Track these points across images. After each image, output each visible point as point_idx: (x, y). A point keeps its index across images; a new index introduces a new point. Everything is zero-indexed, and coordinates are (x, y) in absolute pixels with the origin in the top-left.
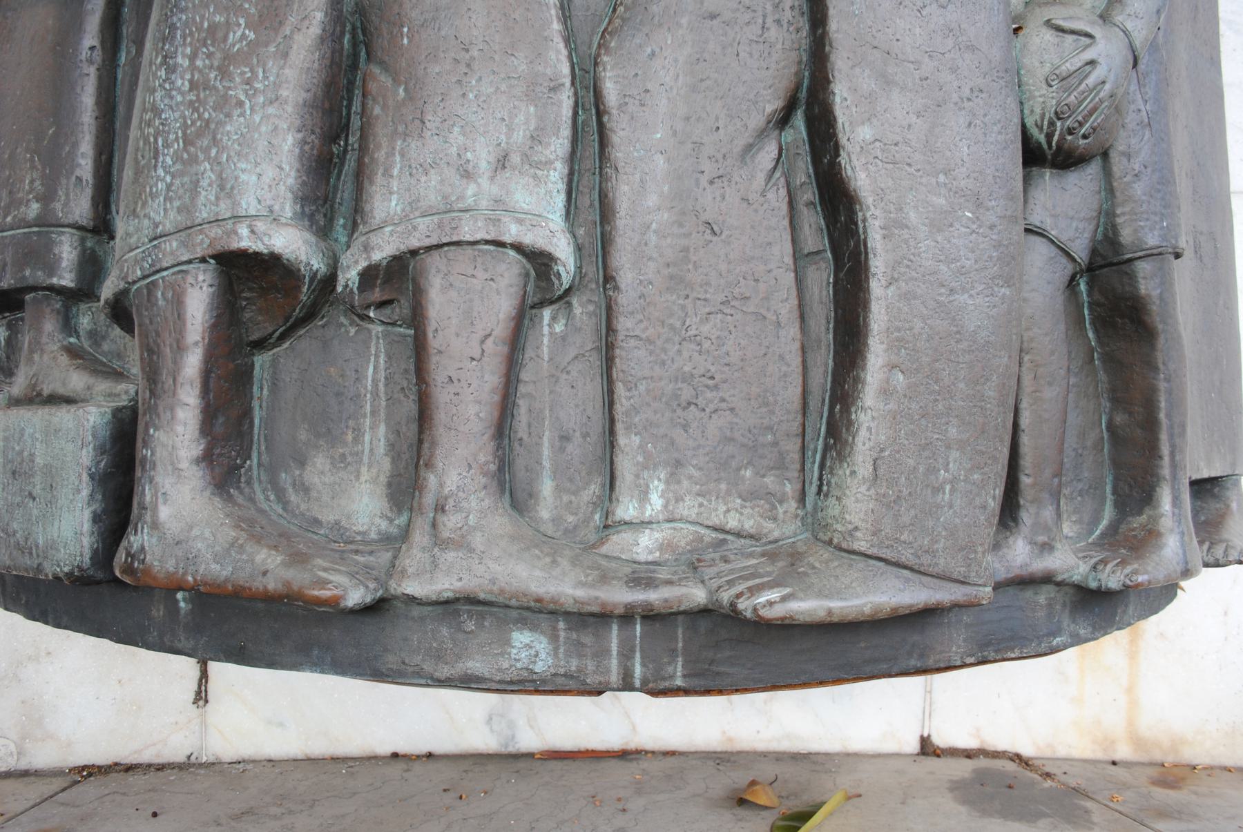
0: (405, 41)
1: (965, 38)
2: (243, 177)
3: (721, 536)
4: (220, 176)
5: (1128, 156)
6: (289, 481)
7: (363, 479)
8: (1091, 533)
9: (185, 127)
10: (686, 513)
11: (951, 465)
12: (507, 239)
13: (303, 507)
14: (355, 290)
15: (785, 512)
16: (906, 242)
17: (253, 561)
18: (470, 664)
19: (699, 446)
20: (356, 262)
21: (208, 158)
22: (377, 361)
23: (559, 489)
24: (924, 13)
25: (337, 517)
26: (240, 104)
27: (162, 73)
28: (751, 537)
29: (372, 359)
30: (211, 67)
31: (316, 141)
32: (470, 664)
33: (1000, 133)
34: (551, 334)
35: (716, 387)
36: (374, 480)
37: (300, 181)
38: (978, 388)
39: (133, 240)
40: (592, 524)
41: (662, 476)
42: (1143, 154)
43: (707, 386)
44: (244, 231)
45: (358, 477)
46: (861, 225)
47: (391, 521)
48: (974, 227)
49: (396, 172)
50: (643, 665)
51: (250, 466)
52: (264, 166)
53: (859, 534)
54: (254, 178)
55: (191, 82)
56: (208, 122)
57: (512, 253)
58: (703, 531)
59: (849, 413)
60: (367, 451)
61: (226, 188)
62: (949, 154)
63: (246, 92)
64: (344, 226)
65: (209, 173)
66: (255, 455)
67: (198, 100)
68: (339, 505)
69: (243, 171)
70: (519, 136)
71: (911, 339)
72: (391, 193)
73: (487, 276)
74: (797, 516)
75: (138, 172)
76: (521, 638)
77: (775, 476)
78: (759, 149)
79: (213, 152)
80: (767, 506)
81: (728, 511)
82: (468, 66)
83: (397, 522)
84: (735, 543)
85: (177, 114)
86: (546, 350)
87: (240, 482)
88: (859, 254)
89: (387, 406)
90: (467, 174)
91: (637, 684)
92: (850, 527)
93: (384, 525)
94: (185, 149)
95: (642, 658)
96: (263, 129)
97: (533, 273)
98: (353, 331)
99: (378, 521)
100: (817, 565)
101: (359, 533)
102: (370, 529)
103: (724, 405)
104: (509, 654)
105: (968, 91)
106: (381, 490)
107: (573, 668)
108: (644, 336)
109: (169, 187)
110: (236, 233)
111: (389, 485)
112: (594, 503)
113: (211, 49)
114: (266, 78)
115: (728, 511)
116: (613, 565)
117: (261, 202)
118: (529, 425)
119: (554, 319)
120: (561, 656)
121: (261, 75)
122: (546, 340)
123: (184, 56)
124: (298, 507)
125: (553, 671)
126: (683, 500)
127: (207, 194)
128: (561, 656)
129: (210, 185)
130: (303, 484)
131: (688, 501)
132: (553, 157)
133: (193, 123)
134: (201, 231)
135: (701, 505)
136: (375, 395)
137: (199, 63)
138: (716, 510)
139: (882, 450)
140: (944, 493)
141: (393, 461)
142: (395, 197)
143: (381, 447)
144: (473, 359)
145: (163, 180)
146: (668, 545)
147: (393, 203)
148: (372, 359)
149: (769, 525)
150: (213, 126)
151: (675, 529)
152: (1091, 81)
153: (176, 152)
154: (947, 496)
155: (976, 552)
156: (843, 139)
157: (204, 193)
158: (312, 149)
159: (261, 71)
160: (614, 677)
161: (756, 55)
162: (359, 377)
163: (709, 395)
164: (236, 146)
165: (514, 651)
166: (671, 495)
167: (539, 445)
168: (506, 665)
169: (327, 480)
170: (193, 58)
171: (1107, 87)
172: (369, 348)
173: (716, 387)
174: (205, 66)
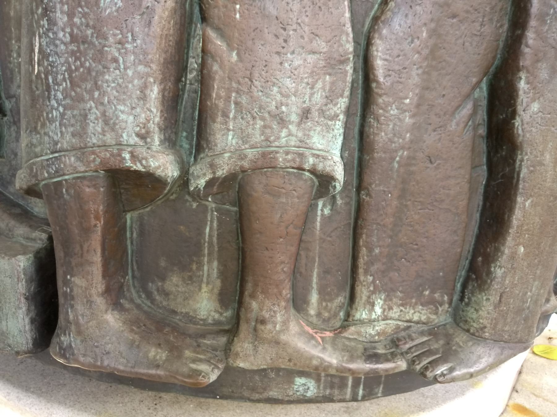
0: (238, 16)
2: (123, 117)
3: (409, 324)
4: (104, 114)
6: (154, 287)
7: (203, 290)
9: (69, 70)
10: (393, 315)
11: (534, 289)
12: (307, 167)
13: (165, 303)
14: (202, 189)
15: (443, 310)
17: (147, 357)
18: (271, 393)
19: (404, 281)
20: (205, 175)
21: (92, 98)
23: (321, 300)
25: (187, 310)
26: (115, 60)
27: (45, 22)
28: (424, 323)
29: (209, 223)
30: (87, 26)
31: (171, 86)
32: (271, 393)
34: (322, 215)
35: (418, 250)
37: (163, 119)
39: (38, 150)
40: (338, 317)
41: (383, 297)
43: (413, 249)
44: (127, 156)
45: (200, 289)
46: (518, 163)
47: (221, 314)
49: (231, 116)
50: (364, 390)
51: (128, 280)
52: (138, 110)
53: (486, 330)
54: (131, 118)
55: (71, 35)
56: (89, 70)
57: (307, 174)
58: (400, 323)
59: (489, 267)
60: (205, 275)
61: (109, 123)
63: (119, 50)
64: (187, 137)
65: (94, 110)
66: (130, 272)
67: (79, 51)
68: (188, 304)
69: (122, 112)
70: (318, 98)
71: (532, 229)
72: (229, 130)
73: (291, 188)
74: (447, 311)
75: (34, 100)
77: (440, 293)
78: (463, 108)
79: (96, 94)
80: (434, 308)
81: (415, 312)
82: (285, 41)
84: (415, 328)
85: (62, 60)
86: (318, 224)
87: (124, 292)
88: (513, 178)
89: (219, 251)
90: (283, 122)
91: (360, 398)
92: (482, 326)
93: (217, 316)
94: (72, 89)
95: (364, 387)
96: (136, 82)
97: (317, 183)
98: (195, 205)
99: (213, 313)
100: (461, 344)
101: (201, 320)
102: (208, 317)
103: (420, 259)
104: (293, 388)
107: (327, 393)
108: (382, 223)
109: (62, 115)
110: (120, 155)
112: (340, 307)
113: (86, 10)
114: (134, 40)
116: (353, 344)
117: (130, 122)
118: (306, 265)
119: (324, 206)
120: (321, 388)
121: (130, 38)
122: (319, 219)
123: (62, 12)
124: (161, 302)
125: (316, 395)
126: (392, 309)
127: (95, 127)
128: (321, 388)
129: (97, 119)
130: (164, 291)
131: (395, 309)
132: (338, 112)
133: (77, 69)
134: (93, 153)
135: (401, 311)
136: (211, 243)
137: (76, 20)
138: (409, 312)
139: (506, 288)
141: (222, 282)
142: (231, 133)
144: (281, 237)
145: (57, 109)
146: (383, 333)
147: (230, 137)
148: (209, 223)
149: (434, 317)
150: (94, 74)
151: (387, 324)
153: (65, 89)
156: (520, 109)
157: (91, 124)
158: (169, 93)
159: (129, 35)
160: (348, 396)
161: (474, 44)
162: (201, 233)
163: (414, 253)
164: (115, 92)
165: (296, 387)
166: (386, 307)
167: (311, 276)
168: (291, 393)
169: (180, 290)
170: (71, 15)
172: (206, 217)
173: (418, 250)
174: (82, 24)
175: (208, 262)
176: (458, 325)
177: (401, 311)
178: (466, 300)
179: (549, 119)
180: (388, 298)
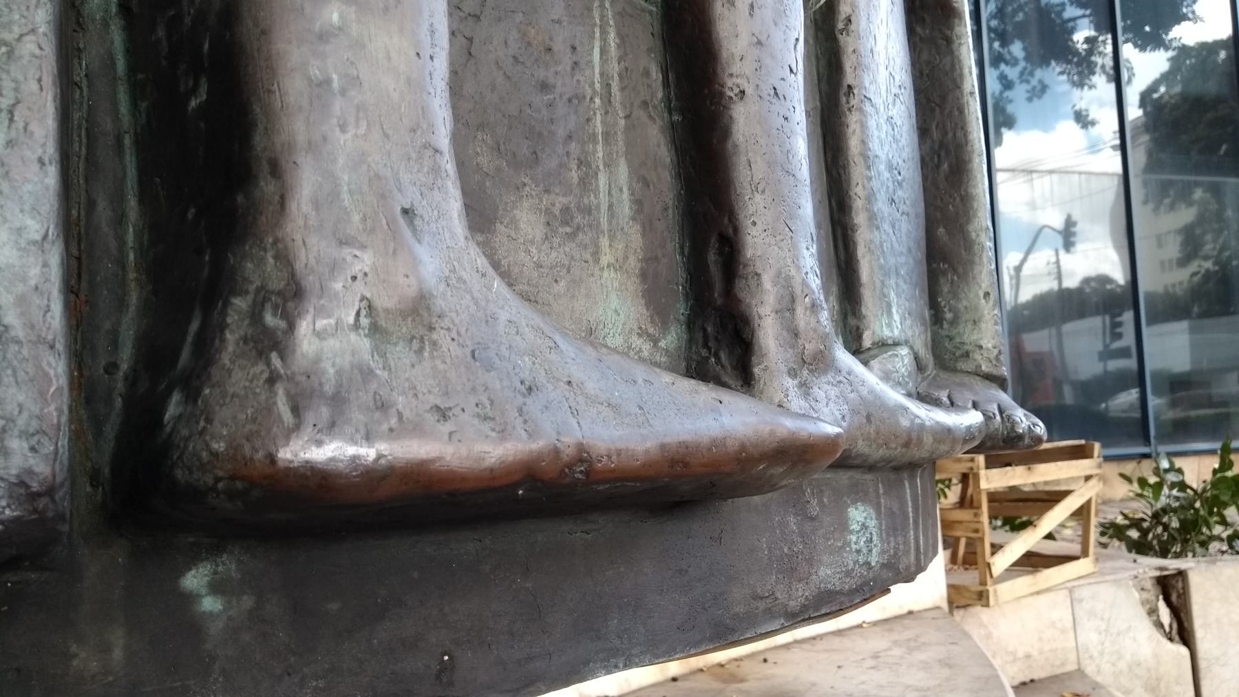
7: (606, 259)
22: (604, 39)
36: (618, 267)
45: (596, 255)
47: (655, 342)
60: (604, 207)
76: (858, 514)
83: (662, 344)
89: (627, 129)
106: (634, 285)
111: (644, 275)
143: (625, 209)
148: (597, 30)
175: (607, 165)
176: (954, 370)
178: (949, 316)
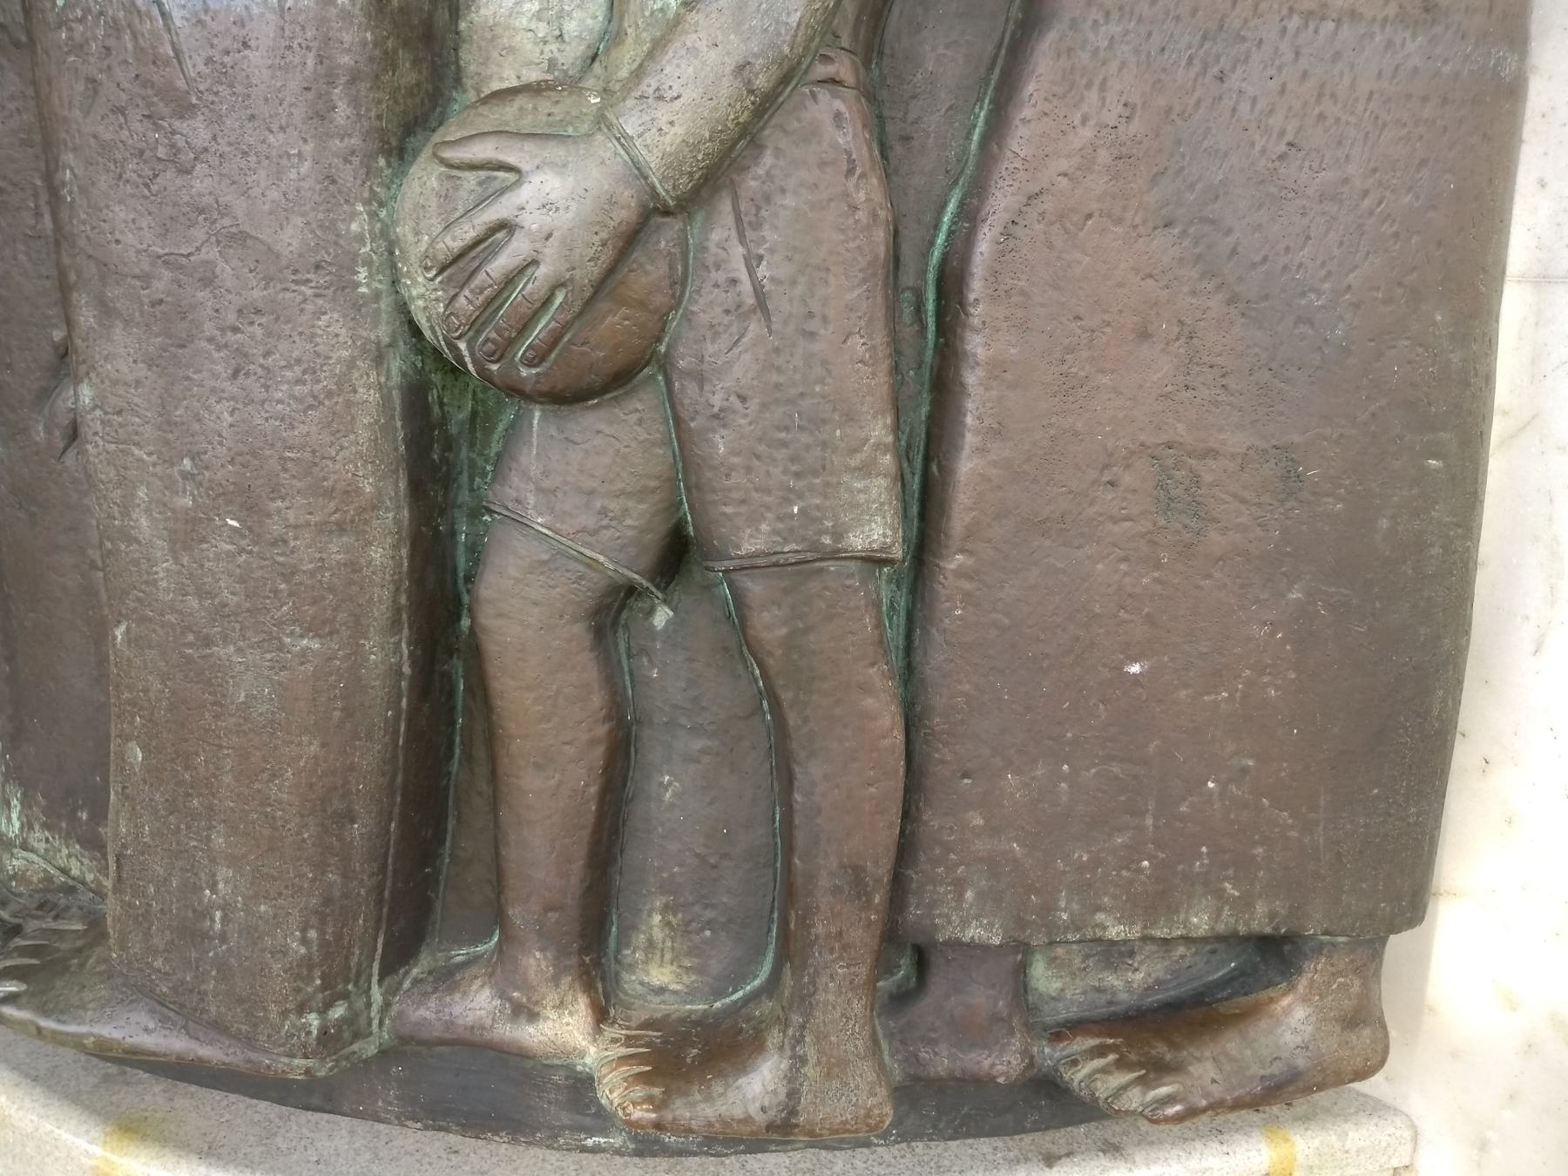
1: (226, 222)
5: (700, 379)
8: (719, 993)
11: (221, 886)
16: (136, 563)
24: (154, 188)
33: (298, 382)
38: (257, 786)
42: (737, 371)
48: (244, 543)
62: (197, 426)
71: (146, 704)
105: (231, 318)
115: (69, 856)
140: (213, 921)
152: (500, 265)
154: (218, 926)
155: (265, 1010)
171: (542, 271)
177: (47, 840)
179: (121, 425)
180: (26, 803)
